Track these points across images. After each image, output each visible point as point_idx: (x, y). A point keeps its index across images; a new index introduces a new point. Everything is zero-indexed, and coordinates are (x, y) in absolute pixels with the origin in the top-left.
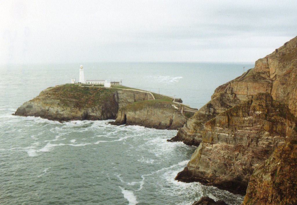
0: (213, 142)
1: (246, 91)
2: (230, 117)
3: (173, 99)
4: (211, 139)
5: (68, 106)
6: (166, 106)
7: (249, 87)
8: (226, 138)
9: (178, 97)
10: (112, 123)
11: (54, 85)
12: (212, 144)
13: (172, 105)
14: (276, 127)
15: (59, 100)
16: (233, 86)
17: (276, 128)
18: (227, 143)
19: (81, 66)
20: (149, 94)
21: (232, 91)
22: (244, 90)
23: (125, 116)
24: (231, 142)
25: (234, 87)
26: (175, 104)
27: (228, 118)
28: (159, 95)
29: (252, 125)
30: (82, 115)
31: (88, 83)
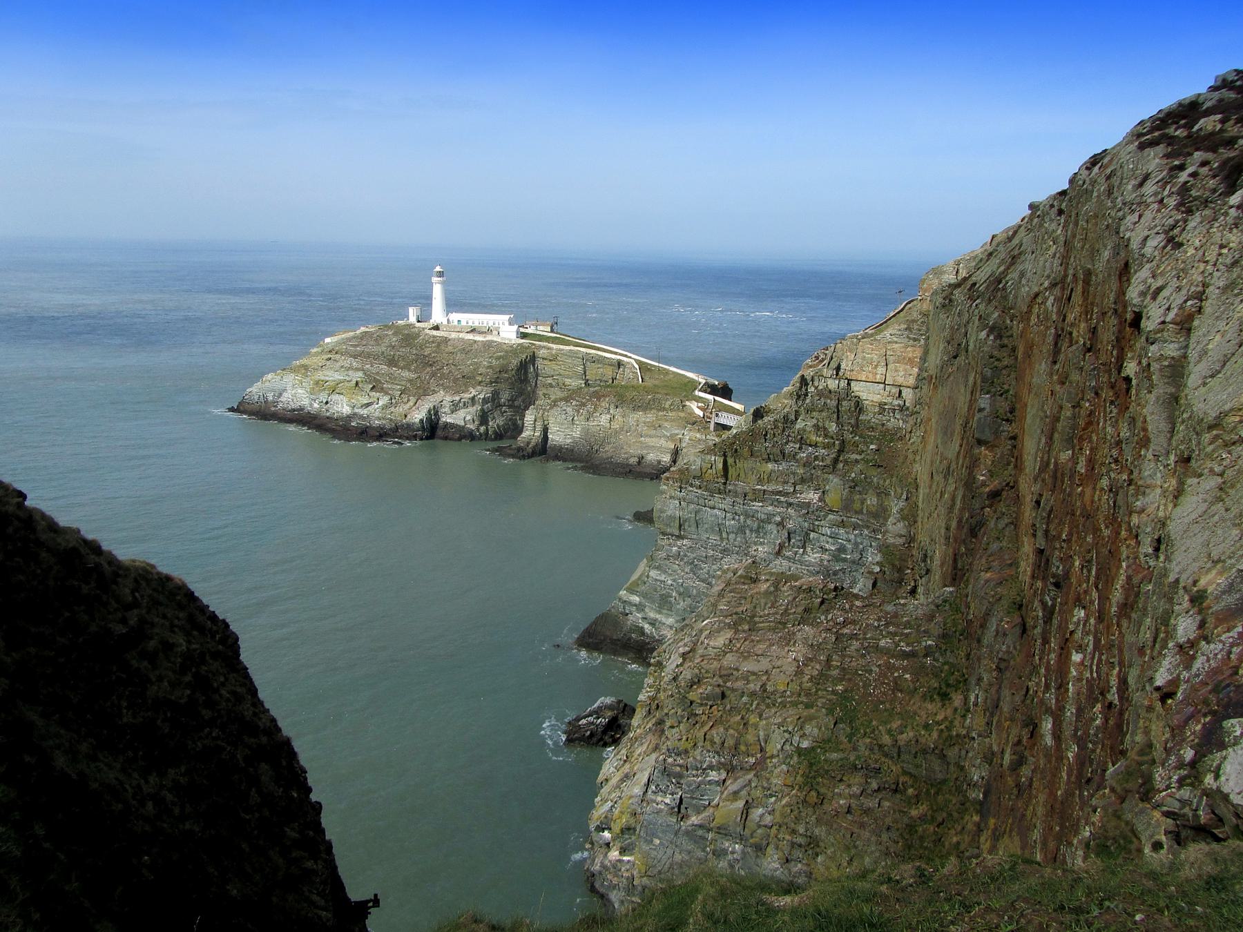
0: (682, 533)
1: (881, 370)
2: (730, 461)
3: (700, 384)
4: (677, 525)
5: (387, 394)
6: (667, 406)
7: (891, 359)
10: (494, 450)
12: (680, 537)
13: (688, 403)
14: (863, 502)
15: (360, 374)
16: (843, 355)
17: (863, 503)
18: (722, 539)
19: (438, 269)
21: (838, 368)
22: (876, 366)
23: (545, 430)
25: (847, 357)
26: (698, 399)
27: (725, 463)
30: (421, 421)
31: (456, 323)
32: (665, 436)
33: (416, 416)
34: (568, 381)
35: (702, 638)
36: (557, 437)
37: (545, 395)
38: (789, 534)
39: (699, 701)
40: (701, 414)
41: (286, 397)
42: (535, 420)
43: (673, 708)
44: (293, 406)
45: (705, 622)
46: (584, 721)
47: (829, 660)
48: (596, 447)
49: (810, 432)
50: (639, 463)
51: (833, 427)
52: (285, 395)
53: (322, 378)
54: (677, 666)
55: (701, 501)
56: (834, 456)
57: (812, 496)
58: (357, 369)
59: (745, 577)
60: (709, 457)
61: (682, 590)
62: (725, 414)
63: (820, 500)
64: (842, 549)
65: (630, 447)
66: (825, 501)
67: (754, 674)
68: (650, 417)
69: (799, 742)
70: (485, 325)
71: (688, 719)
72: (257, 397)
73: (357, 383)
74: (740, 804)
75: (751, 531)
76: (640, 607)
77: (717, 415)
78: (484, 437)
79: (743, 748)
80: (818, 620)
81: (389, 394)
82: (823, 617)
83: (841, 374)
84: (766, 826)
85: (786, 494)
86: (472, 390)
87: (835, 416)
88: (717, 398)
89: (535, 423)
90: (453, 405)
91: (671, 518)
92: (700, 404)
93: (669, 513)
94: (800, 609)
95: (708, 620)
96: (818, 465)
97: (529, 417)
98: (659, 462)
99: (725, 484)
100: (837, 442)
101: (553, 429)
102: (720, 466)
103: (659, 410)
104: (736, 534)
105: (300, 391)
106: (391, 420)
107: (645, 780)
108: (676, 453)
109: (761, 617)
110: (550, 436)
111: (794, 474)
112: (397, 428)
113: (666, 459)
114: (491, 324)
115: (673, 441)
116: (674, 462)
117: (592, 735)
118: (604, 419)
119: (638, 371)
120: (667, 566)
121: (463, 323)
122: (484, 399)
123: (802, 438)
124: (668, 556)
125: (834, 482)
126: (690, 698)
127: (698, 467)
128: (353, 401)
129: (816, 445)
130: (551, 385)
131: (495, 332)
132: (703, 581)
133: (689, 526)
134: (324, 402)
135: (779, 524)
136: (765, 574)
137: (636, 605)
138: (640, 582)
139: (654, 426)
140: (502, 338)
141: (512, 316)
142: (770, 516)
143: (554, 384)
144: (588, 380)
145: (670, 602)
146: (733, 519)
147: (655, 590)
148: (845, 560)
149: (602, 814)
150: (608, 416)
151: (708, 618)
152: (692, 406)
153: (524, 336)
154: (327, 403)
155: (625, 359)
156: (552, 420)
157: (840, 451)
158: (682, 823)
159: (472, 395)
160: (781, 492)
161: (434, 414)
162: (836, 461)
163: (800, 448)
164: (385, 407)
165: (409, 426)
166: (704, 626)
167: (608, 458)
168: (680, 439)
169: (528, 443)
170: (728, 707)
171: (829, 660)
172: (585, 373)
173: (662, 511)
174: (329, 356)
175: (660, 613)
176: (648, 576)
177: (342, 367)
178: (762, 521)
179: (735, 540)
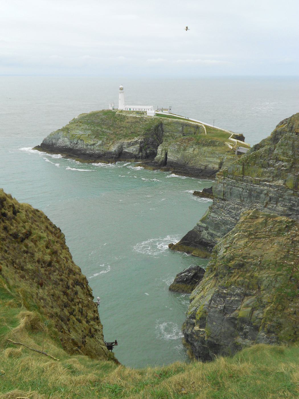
2: (246, 167)
4: (222, 194)
8: (240, 194)
9: (238, 133)
11: (88, 111)
12: (224, 200)
13: (226, 143)
19: (121, 87)
20: (202, 126)
21: (292, 127)
24: (245, 199)
26: (231, 141)
27: (243, 168)
28: (214, 129)
29: (272, 180)
30: (115, 151)
31: (129, 110)
32: (216, 157)
33: (113, 149)
34: (175, 134)
35: (234, 241)
36: (171, 157)
37: (166, 140)
38: (270, 198)
39: (233, 267)
40: (232, 147)
41: (60, 141)
42: (162, 151)
43: (222, 270)
44: (63, 145)
45: (236, 235)
46: (183, 274)
47: (288, 252)
48: (187, 162)
49: (280, 155)
50: (205, 168)
51: (290, 153)
52: (60, 140)
53: (75, 133)
54: (224, 252)
55: (233, 184)
56: (290, 165)
57: (280, 182)
58: (89, 130)
59: (253, 216)
60: (236, 165)
61: (224, 221)
62: (241, 147)
63: (284, 184)
64: (294, 205)
65: (201, 162)
66: (286, 185)
67: (256, 256)
68: (210, 149)
69: (275, 284)
70: (141, 110)
71: (228, 274)
72: (48, 141)
73: (89, 135)
74: (249, 309)
75: (254, 197)
76: (207, 229)
77: (238, 148)
78: (141, 158)
79: (251, 287)
80: (284, 235)
81: (102, 140)
82: (286, 233)
83: (293, 130)
84: (260, 318)
85: (269, 182)
86: (136, 138)
87: (292, 148)
88: (239, 141)
89: (162, 152)
90: (128, 144)
91: (220, 191)
92: (231, 143)
93: (219, 189)
94: (277, 230)
95: (237, 234)
96: (284, 169)
97: (159, 149)
98: (214, 168)
99: (243, 177)
100: (292, 159)
101: (169, 154)
102: (241, 169)
103: (213, 146)
104: (247, 198)
105: (66, 139)
106: (102, 150)
107: (210, 298)
108: (221, 164)
109: (260, 233)
110: (168, 157)
111: (273, 173)
112: (104, 155)
113: (217, 167)
114: (143, 110)
115: (220, 159)
116: (220, 168)
117: (187, 280)
118: (191, 150)
119: (205, 129)
120: (218, 211)
121: (132, 110)
122: (140, 142)
123: (277, 157)
124: (219, 207)
125: (290, 175)
126: (229, 266)
127: (232, 170)
128: (87, 143)
129: (283, 161)
130: (168, 136)
131: (145, 113)
132: (233, 218)
133: (228, 195)
134: (76, 143)
135: (265, 194)
136: (261, 215)
137: (204, 227)
138: (206, 218)
139: (212, 153)
140: (149, 116)
141: (152, 106)
142: (262, 191)
143: (170, 135)
144: (184, 134)
145: (219, 227)
146: (246, 192)
147: (213, 221)
148: (294, 210)
149: (192, 312)
150: (192, 149)
151: (237, 233)
152: (228, 144)
153: (157, 115)
154: (77, 143)
155: (199, 124)
156: (169, 150)
157: (294, 163)
158: (225, 316)
159: (136, 140)
160: (267, 180)
161: (121, 148)
162: (291, 167)
163: (276, 162)
164: (100, 145)
165: (110, 153)
166: (235, 236)
167: (192, 166)
168: (223, 158)
169: (159, 160)
170: (245, 270)
171: (288, 252)
172: (183, 130)
173: (216, 188)
174: (77, 124)
175: (215, 231)
176: (210, 216)
177: (83, 128)
178: (259, 193)
179: (247, 201)
